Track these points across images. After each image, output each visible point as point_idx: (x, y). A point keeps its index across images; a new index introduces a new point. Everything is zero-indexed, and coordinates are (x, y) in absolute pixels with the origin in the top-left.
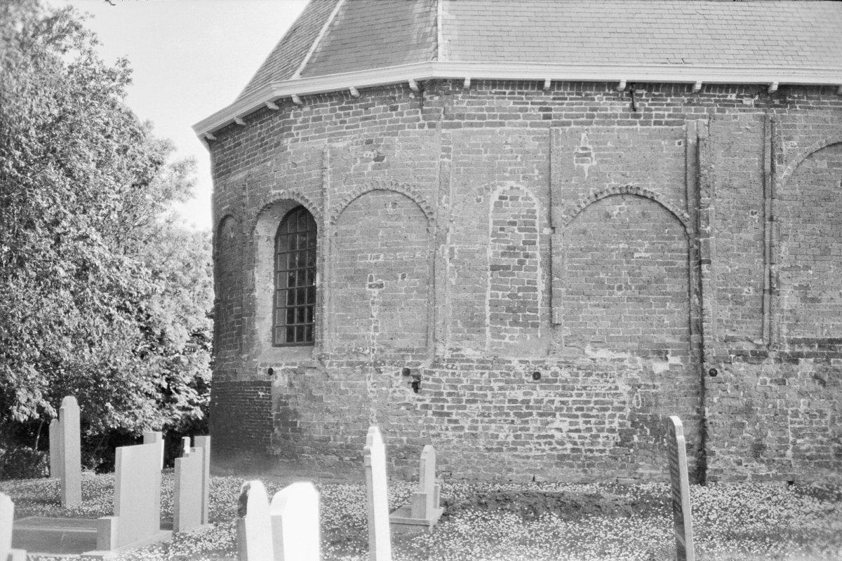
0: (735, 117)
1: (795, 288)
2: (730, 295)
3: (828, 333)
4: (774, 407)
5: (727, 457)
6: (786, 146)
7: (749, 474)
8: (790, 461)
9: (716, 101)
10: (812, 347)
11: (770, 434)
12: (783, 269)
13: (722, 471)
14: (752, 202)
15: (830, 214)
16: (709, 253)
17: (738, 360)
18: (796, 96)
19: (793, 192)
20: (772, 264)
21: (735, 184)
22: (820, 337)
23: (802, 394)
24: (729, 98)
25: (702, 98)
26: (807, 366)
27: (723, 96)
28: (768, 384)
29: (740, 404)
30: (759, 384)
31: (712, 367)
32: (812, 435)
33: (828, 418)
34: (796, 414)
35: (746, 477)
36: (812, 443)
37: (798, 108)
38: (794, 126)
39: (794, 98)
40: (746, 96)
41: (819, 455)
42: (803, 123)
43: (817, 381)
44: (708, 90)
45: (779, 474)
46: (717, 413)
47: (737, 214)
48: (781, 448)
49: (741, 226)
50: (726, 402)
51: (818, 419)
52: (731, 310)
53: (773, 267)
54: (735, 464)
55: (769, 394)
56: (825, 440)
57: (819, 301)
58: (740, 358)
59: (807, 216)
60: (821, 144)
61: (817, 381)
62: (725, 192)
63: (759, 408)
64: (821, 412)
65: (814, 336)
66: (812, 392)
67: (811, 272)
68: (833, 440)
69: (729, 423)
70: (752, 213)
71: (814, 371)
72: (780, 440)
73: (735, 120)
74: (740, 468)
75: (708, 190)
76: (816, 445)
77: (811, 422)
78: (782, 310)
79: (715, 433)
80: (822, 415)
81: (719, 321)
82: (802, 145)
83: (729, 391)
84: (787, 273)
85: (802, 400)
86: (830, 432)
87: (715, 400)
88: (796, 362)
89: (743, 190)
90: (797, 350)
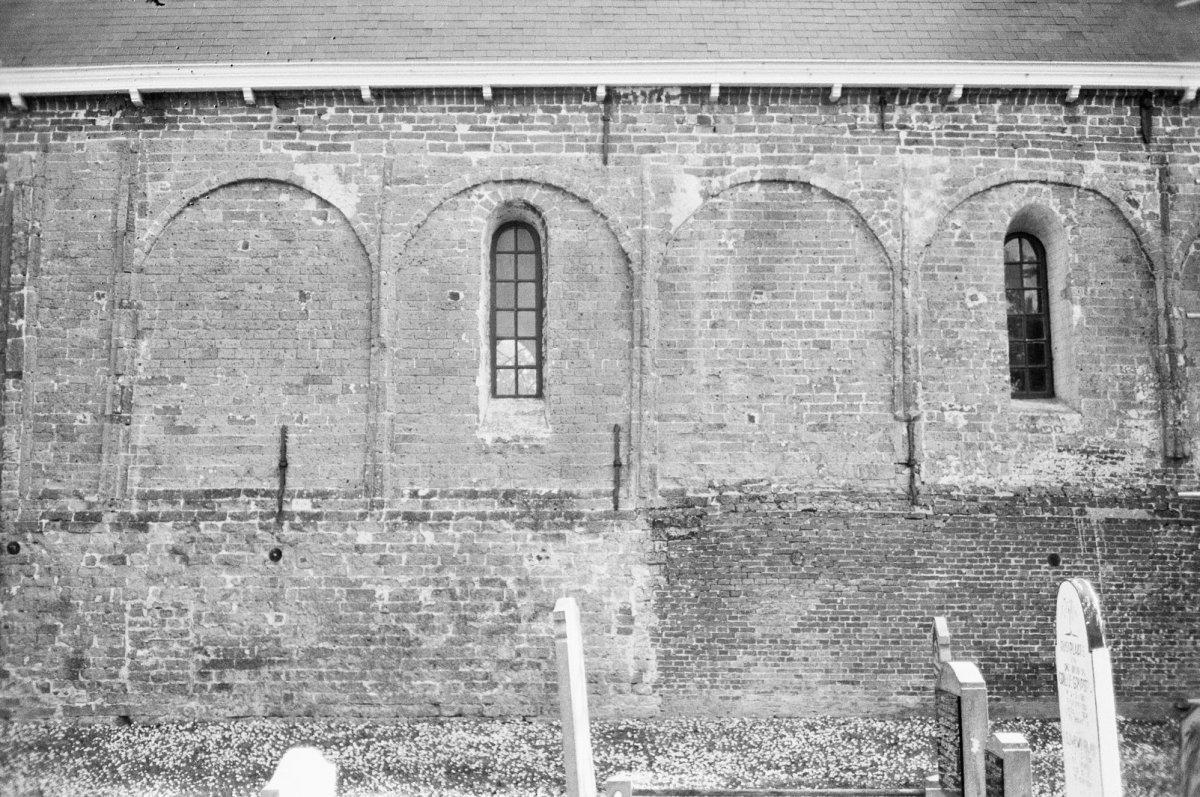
0: (80, 146)
1: (157, 411)
2: (54, 426)
3: (205, 481)
4: (105, 599)
5: (27, 680)
6: (152, 190)
7: (58, 705)
8: (124, 685)
9: (54, 123)
10: (174, 504)
11: (96, 643)
12: (141, 383)
13: (17, 702)
14: (99, 279)
15: (222, 294)
16: (19, 359)
17: (54, 527)
18: (180, 109)
19: (163, 261)
20: (118, 375)
21: (73, 251)
22: (193, 488)
23: (153, 578)
24: (73, 117)
25: (33, 119)
26: (163, 534)
27: (64, 115)
28: (98, 564)
29: (52, 596)
30: (83, 564)
31: (13, 539)
32: (164, 643)
33: (190, 615)
34: (137, 611)
35: (52, 712)
36: (162, 655)
37: (181, 129)
38: (168, 157)
39: (177, 112)
40: (102, 113)
41: (171, 674)
42: (183, 152)
43: (178, 558)
44: (43, 106)
45: (106, 705)
46: (15, 612)
47: (73, 298)
48: (112, 664)
49: (79, 317)
50: (31, 593)
51: (174, 618)
52: (55, 449)
53: (121, 380)
54: (37, 691)
55: (99, 580)
56: (182, 650)
57: (194, 431)
58: (58, 524)
59: (183, 299)
60: (209, 183)
61: (178, 558)
62: (58, 264)
63: (81, 603)
64: (178, 606)
65: (182, 487)
66: (167, 575)
67: (184, 386)
68: (195, 649)
69: (34, 626)
70: (99, 297)
71: (173, 542)
72: (112, 652)
73: (80, 151)
74: (44, 697)
75: (23, 262)
76: (169, 658)
77: (162, 623)
78: (135, 448)
79: (11, 641)
80: (182, 610)
81: (37, 466)
82: (179, 186)
83: (36, 577)
84: (146, 388)
85: (152, 589)
86: (191, 638)
87: (14, 590)
88: (144, 528)
89: (87, 261)
90: (151, 509)
